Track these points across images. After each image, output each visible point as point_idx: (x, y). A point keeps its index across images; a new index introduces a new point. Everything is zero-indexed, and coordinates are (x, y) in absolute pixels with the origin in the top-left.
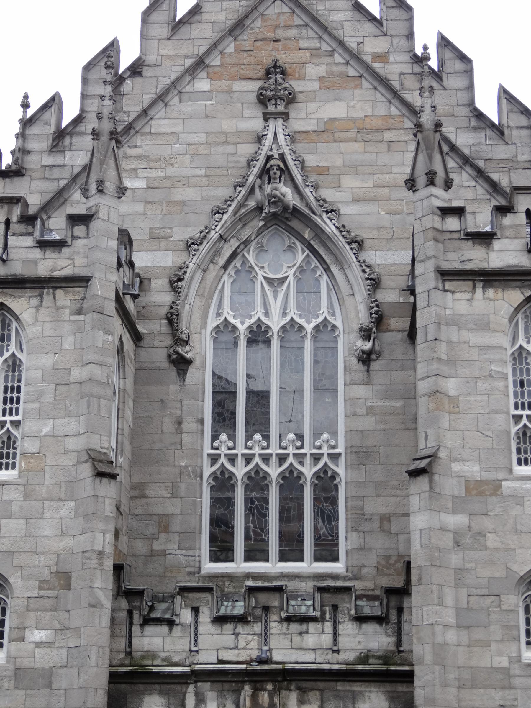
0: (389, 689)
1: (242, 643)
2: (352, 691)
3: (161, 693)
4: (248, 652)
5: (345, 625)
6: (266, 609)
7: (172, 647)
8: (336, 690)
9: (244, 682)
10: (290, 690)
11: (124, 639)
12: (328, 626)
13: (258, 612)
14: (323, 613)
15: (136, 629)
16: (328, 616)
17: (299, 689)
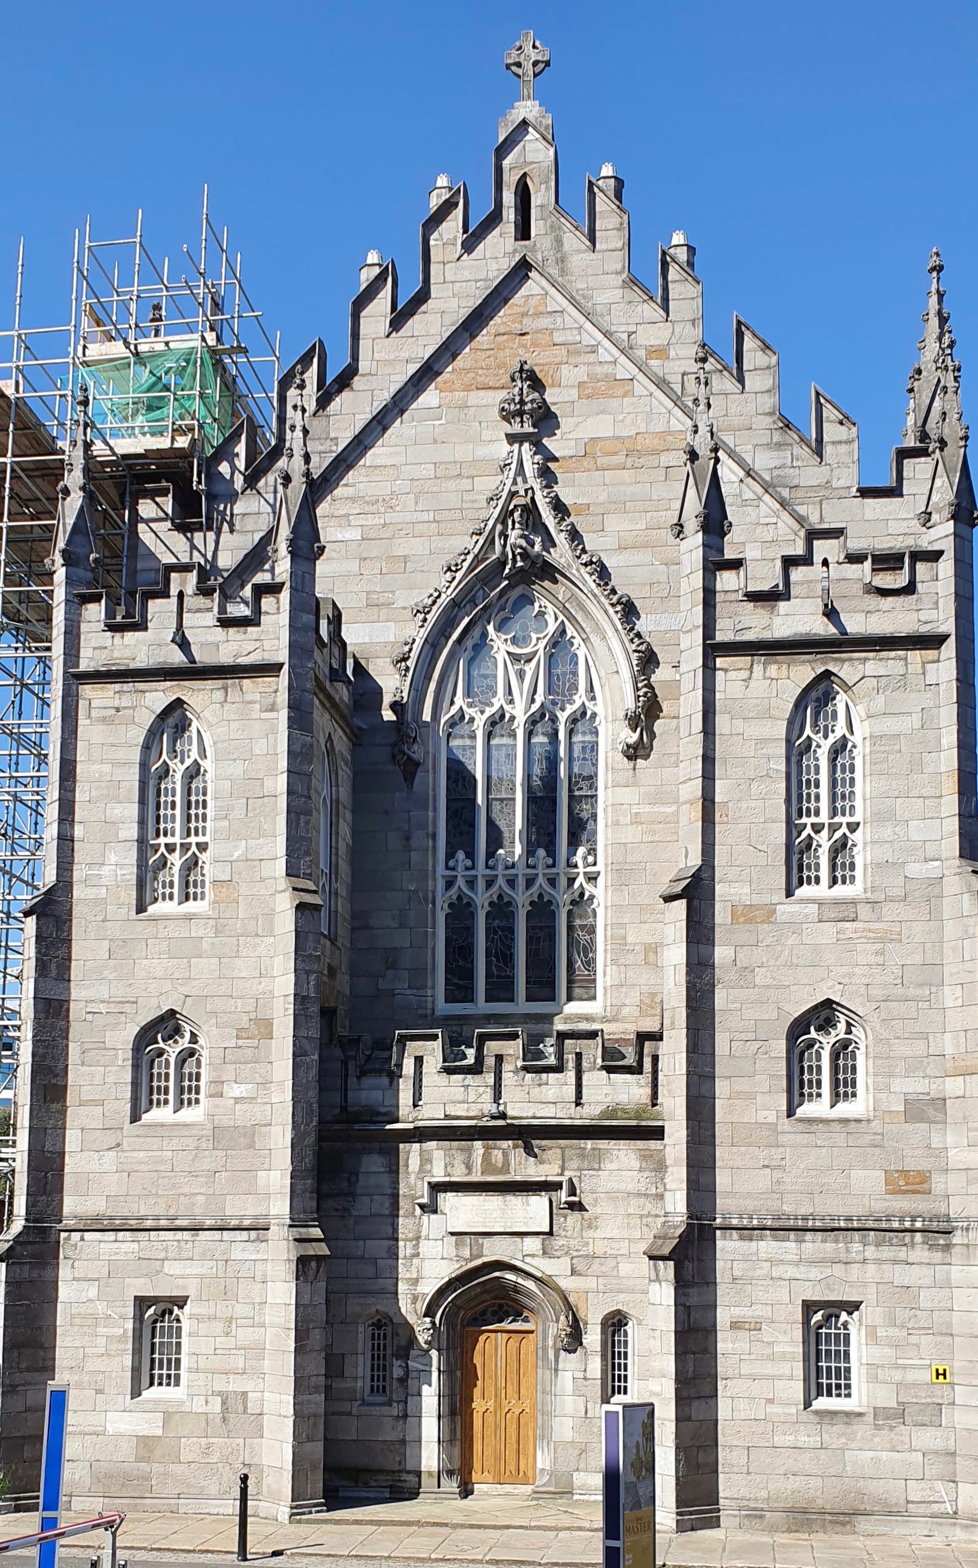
1: (472, 1097)
4: (479, 1106)
15: (352, 1081)
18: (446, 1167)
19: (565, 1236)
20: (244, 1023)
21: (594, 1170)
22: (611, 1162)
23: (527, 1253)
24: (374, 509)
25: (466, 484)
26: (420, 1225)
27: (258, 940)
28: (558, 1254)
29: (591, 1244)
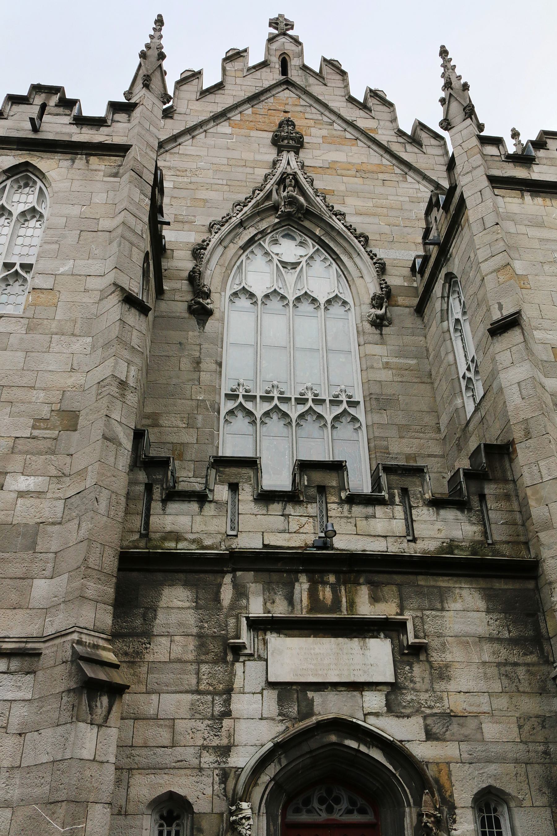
0: (484, 586)
1: (294, 526)
2: (437, 587)
3: (186, 584)
4: (303, 537)
5: (419, 510)
6: (322, 490)
7: (204, 528)
8: (418, 585)
9: (299, 572)
10: (360, 584)
11: (139, 518)
12: (399, 511)
13: (313, 491)
14: (392, 496)
15: (156, 506)
16: (397, 500)
17: (369, 583)
18: (265, 604)
19: (413, 689)
20: (45, 412)
21: (437, 610)
22: (455, 601)
23: (370, 710)
24: (184, 174)
25: (249, 170)
26: (232, 674)
27: (74, 339)
28: (408, 711)
29: (445, 698)
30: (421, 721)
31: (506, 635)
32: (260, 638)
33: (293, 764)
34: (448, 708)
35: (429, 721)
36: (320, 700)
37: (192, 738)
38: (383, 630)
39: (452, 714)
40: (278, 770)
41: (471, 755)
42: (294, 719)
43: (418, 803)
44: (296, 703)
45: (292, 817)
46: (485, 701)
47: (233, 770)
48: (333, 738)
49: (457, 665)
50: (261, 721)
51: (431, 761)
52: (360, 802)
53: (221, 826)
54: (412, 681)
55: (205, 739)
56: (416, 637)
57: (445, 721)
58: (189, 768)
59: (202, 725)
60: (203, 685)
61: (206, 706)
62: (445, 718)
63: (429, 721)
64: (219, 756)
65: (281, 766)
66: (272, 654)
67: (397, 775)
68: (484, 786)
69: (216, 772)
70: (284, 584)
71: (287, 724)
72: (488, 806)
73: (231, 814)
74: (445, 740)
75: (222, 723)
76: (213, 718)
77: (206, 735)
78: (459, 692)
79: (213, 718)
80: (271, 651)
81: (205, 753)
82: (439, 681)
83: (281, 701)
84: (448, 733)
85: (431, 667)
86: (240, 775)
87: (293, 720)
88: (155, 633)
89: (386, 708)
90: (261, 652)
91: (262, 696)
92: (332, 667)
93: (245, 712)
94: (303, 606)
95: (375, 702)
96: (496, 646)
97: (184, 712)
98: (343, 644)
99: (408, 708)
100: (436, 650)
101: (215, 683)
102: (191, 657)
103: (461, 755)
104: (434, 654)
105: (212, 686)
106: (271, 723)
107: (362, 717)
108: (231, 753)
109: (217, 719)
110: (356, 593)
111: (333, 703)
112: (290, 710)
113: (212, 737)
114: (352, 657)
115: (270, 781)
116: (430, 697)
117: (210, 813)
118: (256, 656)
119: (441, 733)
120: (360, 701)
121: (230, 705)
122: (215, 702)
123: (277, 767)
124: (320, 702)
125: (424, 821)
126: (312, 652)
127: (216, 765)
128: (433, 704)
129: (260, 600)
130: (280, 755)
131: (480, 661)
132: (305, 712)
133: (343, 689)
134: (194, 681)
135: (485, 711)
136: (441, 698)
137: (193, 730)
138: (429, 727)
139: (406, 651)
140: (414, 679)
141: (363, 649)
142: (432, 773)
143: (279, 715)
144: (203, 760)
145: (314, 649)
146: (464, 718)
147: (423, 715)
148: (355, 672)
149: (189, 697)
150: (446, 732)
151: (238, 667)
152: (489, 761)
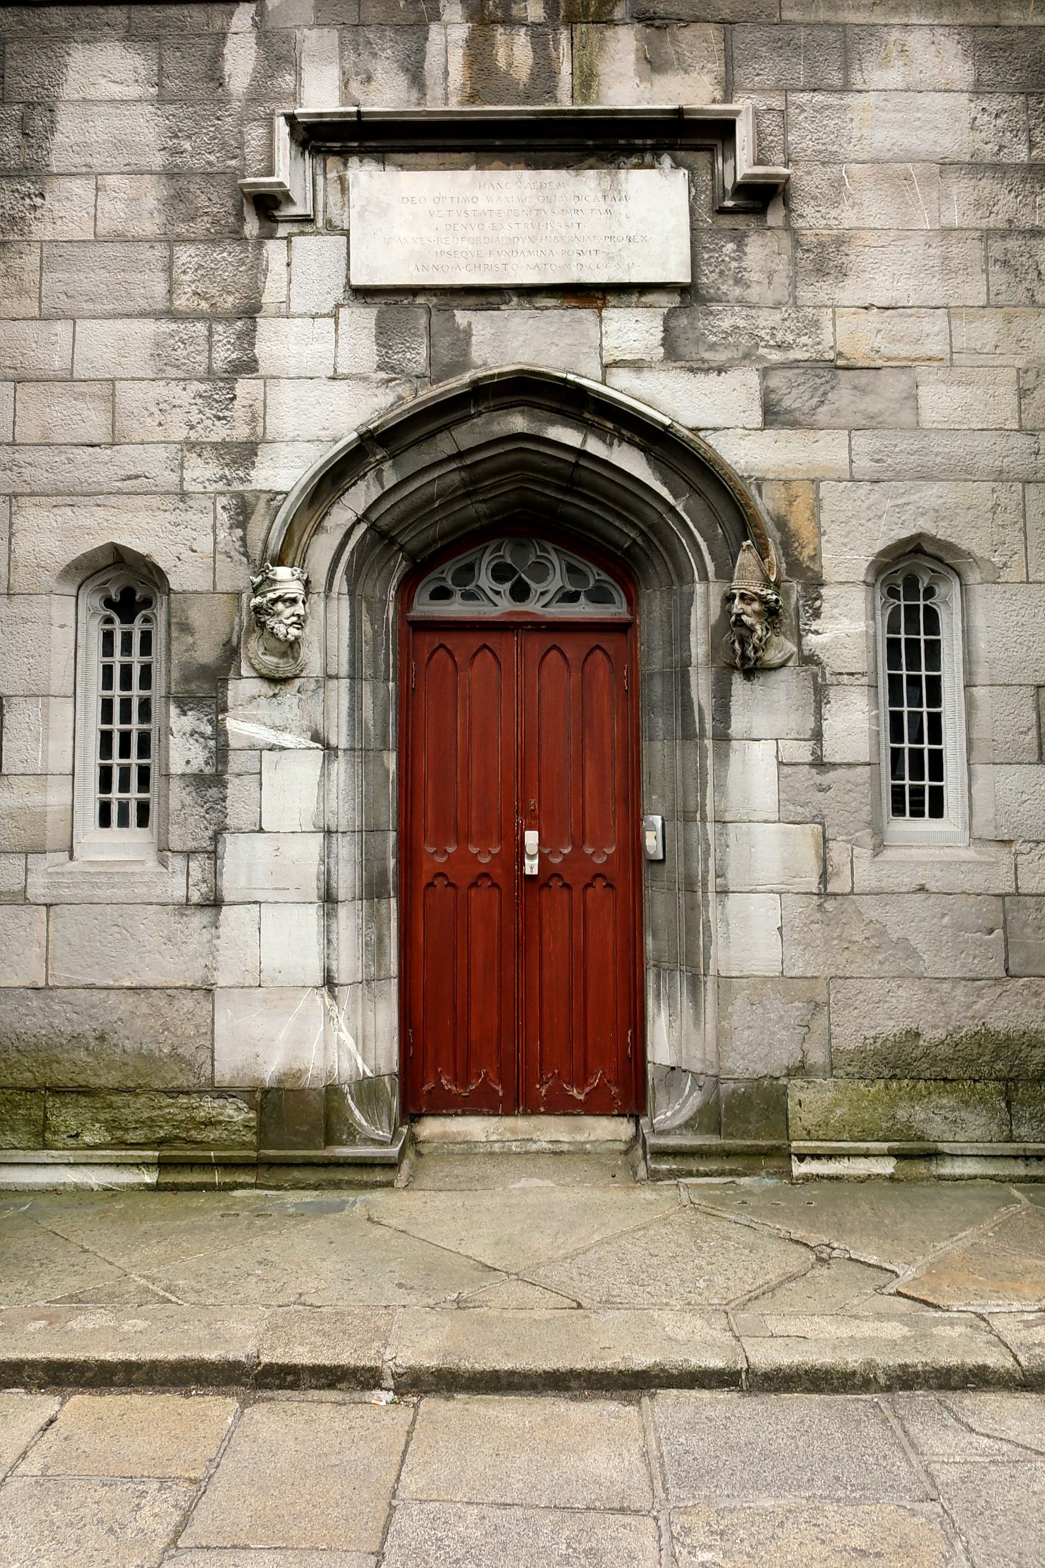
0: (975, 20)
2: (838, 25)
3: (130, 36)
8: (782, 22)
10: (611, 23)
19: (741, 302)
21: (831, 90)
22: (885, 63)
23: (618, 356)
26: (258, 269)
30: (753, 379)
31: (1021, 154)
32: (332, 175)
33: (416, 484)
34: (831, 348)
35: (776, 381)
36: (489, 331)
37: (160, 424)
38: (671, 148)
39: (840, 363)
40: (374, 498)
41: (878, 461)
42: (418, 377)
43: (725, 573)
44: (425, 340)
45: (426, 608)
46: (936, 329)
47: (264, 497)
48: (518, 423)
49: (870, 238)
50: (333, 383)
51: (771, 476)
52: (595, 575)
53: (237, 620)
54: (738, 282)
55: (192, 427)
56: (759, 162)
57: (819, 381)
58: (155, 493)
59: (184, 395)
60: (184, 297)
61: (192, 349)
62: (821, 372)
63: (776, 381)
64: (227, 465)
65: (383, 488)
66: (361, 215)
67: (679, 509)
68: (905, 534)
69: (223, 501)
70: (400, 28)
71: (399, 389)
72: (911, 585)
73: (256, 590)
74: (812, 427)
75: (232, 389)
76: (210, 375)
77: (195, 418)
78: (866, 308)
79: (210, 375)
80: (358, 208)
81: (192, 459)
82: (813, 280)
83: (383, 333)
84: (823, 409)
85: (797, 244)
86: (280, 507)
87: (415, 380)
88: (55, 170)
89: (662, 350)
90: (334, 212)
91: (336, 323)
92: (520, 246)
93: (292, 362)
94: (451, 88)
95: (635, 335)
96: (988, 185)
97: (137, 363)
98: (554, 186)
99: (721, 348)
100: (814, 198)
101: (213, 291)
102: (150, 227)
103: (852, 461)
104: (808, 210)
105: (206, 299)
106: (359, 387)
107: (598, 373)
108: (257, 460)
109: (222, 379)
110: (601, 49)
111: (521, 338)
112: (408, 355)
113: (209, 423)
114: (576, 218)
115: (358, 521)
116: (784, 320)
117: (208, 592)
118: (320, 223)
119: (806, 409)
120: (594, 332)
121: (254, 344)
122: (216, 337)
123: (373, 489)
124: (488, 336)
125: (735, 610)
126: (470, 207)
127: (220, 486)
128: (790, 338)
129: (332, 74)
130: (380, 462)
131: (937, 227)
132: (446, 360)
133: (551, 302)
134: (160, 288)
135: (930, 354)
136: (816, 324)
137: (161, 406)
138: (773, 396)
139: (729, 203)
140: (746, 275)
141: (608, 199)
142: (770, 505)
143: (380, 368)
144: (188, 475)
145: (475, 200)
146: (872, 373)
147: (760, 367)
148: (583, 259)
149: (149, 327)
150: (817, 407)
151: (274, 251)
152: (925, 476)
